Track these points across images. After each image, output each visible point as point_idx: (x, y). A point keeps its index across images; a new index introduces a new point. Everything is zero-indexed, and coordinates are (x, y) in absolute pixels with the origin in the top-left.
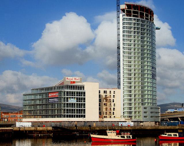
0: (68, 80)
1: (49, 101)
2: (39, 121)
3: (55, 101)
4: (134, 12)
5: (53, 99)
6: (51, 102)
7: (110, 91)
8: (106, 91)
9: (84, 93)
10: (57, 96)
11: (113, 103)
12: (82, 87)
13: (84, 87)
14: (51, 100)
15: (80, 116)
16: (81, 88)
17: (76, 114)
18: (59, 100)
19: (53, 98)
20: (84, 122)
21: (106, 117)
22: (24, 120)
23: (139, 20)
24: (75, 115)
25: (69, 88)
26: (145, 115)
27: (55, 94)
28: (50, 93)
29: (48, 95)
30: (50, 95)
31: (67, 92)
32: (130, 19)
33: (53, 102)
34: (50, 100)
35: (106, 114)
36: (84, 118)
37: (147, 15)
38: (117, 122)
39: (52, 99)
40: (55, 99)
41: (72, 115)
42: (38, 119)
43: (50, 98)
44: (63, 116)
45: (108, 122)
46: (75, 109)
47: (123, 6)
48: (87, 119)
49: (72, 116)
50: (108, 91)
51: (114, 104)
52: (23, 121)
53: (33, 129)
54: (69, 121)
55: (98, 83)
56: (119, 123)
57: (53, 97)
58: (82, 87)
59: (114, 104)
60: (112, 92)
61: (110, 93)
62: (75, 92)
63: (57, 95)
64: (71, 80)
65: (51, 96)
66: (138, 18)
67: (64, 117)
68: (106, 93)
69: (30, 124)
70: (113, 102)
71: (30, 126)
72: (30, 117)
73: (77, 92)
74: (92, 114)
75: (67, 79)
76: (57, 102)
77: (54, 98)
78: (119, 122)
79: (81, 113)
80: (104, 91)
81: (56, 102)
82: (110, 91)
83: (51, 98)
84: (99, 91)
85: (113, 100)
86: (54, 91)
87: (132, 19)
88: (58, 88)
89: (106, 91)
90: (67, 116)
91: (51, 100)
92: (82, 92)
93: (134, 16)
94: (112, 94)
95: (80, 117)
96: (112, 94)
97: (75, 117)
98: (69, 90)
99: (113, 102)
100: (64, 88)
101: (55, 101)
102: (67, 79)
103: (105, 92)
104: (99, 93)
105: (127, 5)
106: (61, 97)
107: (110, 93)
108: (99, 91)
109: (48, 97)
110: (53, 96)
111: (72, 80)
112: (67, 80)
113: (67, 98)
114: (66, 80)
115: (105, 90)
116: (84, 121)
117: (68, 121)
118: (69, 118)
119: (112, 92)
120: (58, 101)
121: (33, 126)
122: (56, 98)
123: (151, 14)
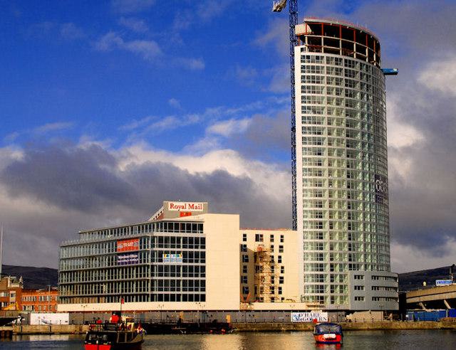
1: (119, 260)
2: (86, 309)
3: (131, 260)
4: (327, 42)
5: (128, 257)
6: (122, 263)
7: (272, 236)
8: (262, 236)
9: (203, 240)
10: (137, 248)
11: (281, 265)
12: (198, 227)
13: (201, 227)
14: (122, 257)
15: (191, 298)
16: (195, 226)
17: (181, 292)
18: (141, 258)
19: (126, 254)
20: (200, 311)
21: (262, 299)
23: (341, 59)
24: (179, 295)
25: (166, 228)
26: (358, 293)
27: (131, 244)
28: (119, 240)
29: (116, 246)
30: (120, 246)
31: (161, 239)
32: (317, 58)
33: (126, 263)
34: (120, 257)
36: (202, 303)
37: (361, 49)
38: (286, 311)
39: (125, 257)
40: (132, 256)
41: (173, 296)
42: (84, 305)
43: (119, 254)
44: (150, 299)
45: (263, 311)
46: (179, 281)
47: (301, 29)
48: (207, 305)
49: (173, 298)
50: (266, 234)
51: (282, 268)
52: (58, 310)
53: (72, 328)
54: (163, 309)
55: (237, 217)
56: (292, 314)
57: (128, 251)
58: (198, 227)
59: (282, 268)
60: (277, 238)
61: (272, 240)
62: (179, 239)
63: (135, 246)
65: (123, 249)
66: (337, 56)
67: (152, 300)
68: (262, 240)
69: (66, 317)
70: (280, 261)
71: (63, 323)
72: (69, 299)
73: (185, 239)
74: (222, 293)
76: (137, 262)
77: (130, 253)
78: (290, 311)
79: (196, 289)
80: (257, 236)
81: (133, 262)
82: (272, 236)
83: (122, 254)
84: (245, 235)
85: (280, 257)
86: (130, 236)
87: (322, 57)
88: (139, 228)
89: (262, 236)
90: (160, 298)
91: (122, 257)
92: (197, 239)
93: (326, 51)
94: (277, 243)
95: (191, 300)
96: (277, 243)
97: (179, 300)
98: (164, 234)
99: (280, 261)
100: (154, 228)
101: (131, 260)
103: (258, 238)
104: (245, 240)
105: (312, 25)
106: (145, 252)
107: (272, 240)
108: (245, 235)
109: (116, 250)
110: (126, 248)
113: (160, 254)
115: (259, 232)
116: (201, 309)
117: (160, 309)
118: (161, 303)
119: (277, 238)
120: (138, 260)
121: (72, 322)
122: (133, 253)
123: (371, 45)
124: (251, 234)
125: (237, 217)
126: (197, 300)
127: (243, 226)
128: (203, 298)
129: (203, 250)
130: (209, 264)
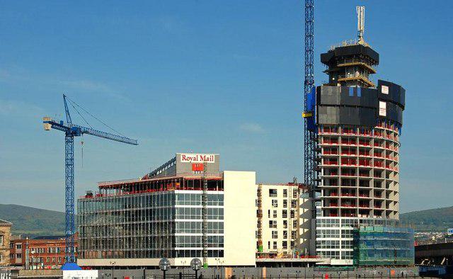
0: (187, 161)
7: (285, 192)
15: (211, 254)
22: (81, 262)
35: (275, 247)
36: (221, 258)
50: (280, 189)
55: (253, 174)
58: (218, 184)
64: (193, 161)
67: (174, 257)
75: (184, 158)
102: (184, 158)
103: (272, 192)
111: (196, 162)
112: (184, 161)
114: (182, 161)
115: (273, 187)
124: (265, 189)
125: (253, 174)
126: (215, 256)
127: (259, 182)
128: (221, 254)
129: (221, 221)
130: (227, 221)
